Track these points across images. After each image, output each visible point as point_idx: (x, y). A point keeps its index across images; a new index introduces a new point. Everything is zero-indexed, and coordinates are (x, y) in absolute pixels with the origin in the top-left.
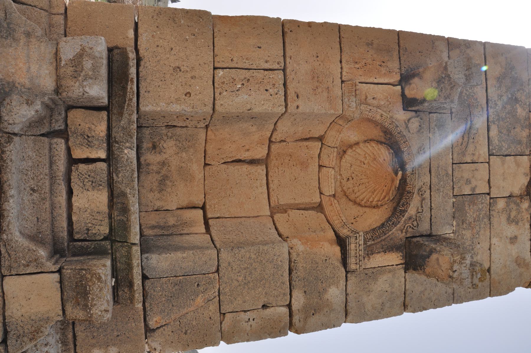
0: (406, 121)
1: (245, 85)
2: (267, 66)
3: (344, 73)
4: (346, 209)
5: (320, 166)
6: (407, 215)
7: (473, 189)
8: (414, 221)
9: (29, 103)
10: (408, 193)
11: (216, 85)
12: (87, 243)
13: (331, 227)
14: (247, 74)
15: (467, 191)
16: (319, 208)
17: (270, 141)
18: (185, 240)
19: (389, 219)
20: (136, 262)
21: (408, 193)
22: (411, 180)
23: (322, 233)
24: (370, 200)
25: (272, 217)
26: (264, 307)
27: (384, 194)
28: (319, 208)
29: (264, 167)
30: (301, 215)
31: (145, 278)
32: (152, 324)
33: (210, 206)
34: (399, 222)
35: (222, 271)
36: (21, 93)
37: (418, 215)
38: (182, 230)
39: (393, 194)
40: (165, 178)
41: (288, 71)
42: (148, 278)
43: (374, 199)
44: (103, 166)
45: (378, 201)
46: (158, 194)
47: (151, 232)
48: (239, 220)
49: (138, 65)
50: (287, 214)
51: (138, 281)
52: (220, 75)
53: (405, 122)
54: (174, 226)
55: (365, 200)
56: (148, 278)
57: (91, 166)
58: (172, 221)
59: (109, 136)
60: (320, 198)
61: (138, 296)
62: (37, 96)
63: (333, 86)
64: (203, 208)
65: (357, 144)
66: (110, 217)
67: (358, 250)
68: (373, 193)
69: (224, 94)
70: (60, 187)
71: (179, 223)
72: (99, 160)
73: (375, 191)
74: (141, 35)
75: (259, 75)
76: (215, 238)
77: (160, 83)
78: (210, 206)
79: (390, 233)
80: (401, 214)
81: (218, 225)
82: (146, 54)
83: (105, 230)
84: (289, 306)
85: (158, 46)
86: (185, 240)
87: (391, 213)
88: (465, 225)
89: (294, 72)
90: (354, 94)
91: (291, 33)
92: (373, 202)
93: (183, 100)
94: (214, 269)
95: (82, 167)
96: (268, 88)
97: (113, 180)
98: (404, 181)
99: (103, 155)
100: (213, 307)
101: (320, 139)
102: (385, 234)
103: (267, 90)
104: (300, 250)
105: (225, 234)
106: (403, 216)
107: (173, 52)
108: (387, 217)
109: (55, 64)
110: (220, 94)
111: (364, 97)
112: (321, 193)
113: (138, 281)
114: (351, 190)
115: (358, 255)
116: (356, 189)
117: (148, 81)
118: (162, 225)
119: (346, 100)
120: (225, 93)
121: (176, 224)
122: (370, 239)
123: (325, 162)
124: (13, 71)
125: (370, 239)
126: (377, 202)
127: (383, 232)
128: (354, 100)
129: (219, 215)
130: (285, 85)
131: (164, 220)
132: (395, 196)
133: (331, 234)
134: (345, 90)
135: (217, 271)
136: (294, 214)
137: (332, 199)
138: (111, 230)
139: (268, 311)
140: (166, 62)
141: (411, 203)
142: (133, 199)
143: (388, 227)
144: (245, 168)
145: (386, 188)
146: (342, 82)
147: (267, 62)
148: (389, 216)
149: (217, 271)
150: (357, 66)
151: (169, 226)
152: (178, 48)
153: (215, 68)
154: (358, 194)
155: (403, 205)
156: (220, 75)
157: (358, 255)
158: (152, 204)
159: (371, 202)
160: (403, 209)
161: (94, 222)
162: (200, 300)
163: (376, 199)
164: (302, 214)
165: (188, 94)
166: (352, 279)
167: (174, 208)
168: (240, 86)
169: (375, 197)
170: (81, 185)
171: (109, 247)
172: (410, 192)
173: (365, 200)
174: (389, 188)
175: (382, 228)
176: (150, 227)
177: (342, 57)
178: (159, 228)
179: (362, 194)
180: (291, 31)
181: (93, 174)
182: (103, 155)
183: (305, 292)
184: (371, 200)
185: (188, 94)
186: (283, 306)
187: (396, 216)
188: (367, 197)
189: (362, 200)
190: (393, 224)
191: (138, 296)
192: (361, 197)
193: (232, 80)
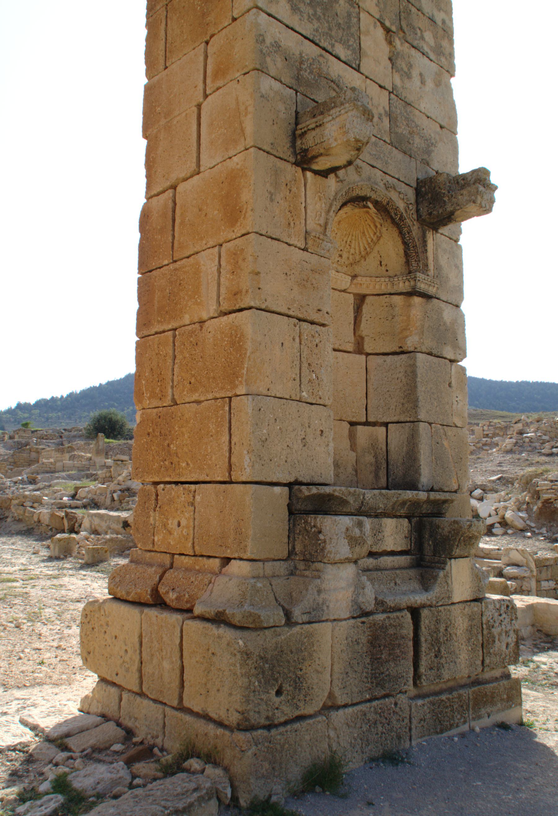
0: (338, 180)
1: (313, 369)
3: (299, 245)
4: (368, 270)
8: (409, 208)
10: (388, 204)
11: (314, 402)
12: (413, 538)
13: (388, 296)
14: (305, 365)
16: (361, 299)
18: (396, 449)
19: (401, 233)
21: (388, 204)
22: (380, 195)
23: (397, 309)
24: (370, 242)
25: (367, 354)
27: (372, 226)
28: (361, 299)
30: (368, 322)
33: (353, 417)
34: (409, 226)
35: (431, 421)
36: (358, 595)
37: (405, 201)
38: (381, 449)
39: (378, 218)
42: (433, 487)
43: (370, 237)
45: (375, 234)
46: (341, 469)
47: (382, 480)
48: (371, 390)
50: (366, 338)
52: (306, 396)
53: (338, 182)
54: (376, 456)
55: (367, 247)
56: (433, 487)
58: (369, 458)
60: (350, 293)
62: (359, 580)
63: (310, 263)
64: (352, 424)
67: (427, 282)
68: (365, 235)
69: (321, 394)
70: (382, 561)
71: (372, 451)
73: (364, 233)
74: (278, 478)
76: (395, 419)
77: (315, 461)
78: (353, 417)
79: (416, 240)
80: (403, 221)
81: (376, 413)
82: (294, 475)
85: (286, 461)
86: (396, 449)
87: (395, 229)
89: (301, 309)
90: (321, 242)
91: (268, 301)
92: (372, 240)
93: (326, 439)
96: (315, 343)
97: (382, 512)
98: (376, 204)
102: (416, 246)
103: (317, 345)
104: (417, 340)
105: (389, 409)
106: (405, 219)
107: (290, 445)
108: (397, 234)
109: (339, 565)
110: (320, 398)
112: (344, 291)
114: (351, 257)
115: (430, 283)
116: (352, 251)
117: (314, 474)
118: (374, 468)
119: (322, 252)
120: (320, 393)
121: (373, 454)
122: (418, 264)
124: (345, 602)
125: (418, 264)
126: (375, 236)
127: (413, 247)
128: (325, 243)
129: (364, 410)
131: (368, 465)
132: (381, 216)
134: (314, 250)
135: (430, 424)
136: (365, 328)
137: (355, 281)
139: (453, 383)
140: (299, 453)
141: (397, 205)
142: (403, 495)
143: (410, 239)
145: (368, 221)
147: (294, 339)
148: (397, 231)
150: (292, 224)
151: (376, 462)
152: (287, 439)
154: (357, 252)
155: (396, 215)
156: (306, 396)
157: (430, 283)
158: (350, 476)
159: (371, 241)
160: (399, 216)
161: (402, 531)
163: (372, 235)
164: (367, 320)
168: (314, 375)
169: (369, 234)
170: (380, 542)
171: (415, 519)
172: (389, 201)
173: (367, 247)
174: (370, 218)
175: (408, 246)
176: (376, 480)
177: (284, 241)
178: (378, 472)
179: (359, 247)
180: (266, 301)
181: (374, 532)
183: (445, 344)
184: (369, 240)
186: (451, 367)
187: (403, 226)
188: (365, 242)
189: (366, 249)
190: (408, 233)
192: (362, 249)
193: (310, 383)
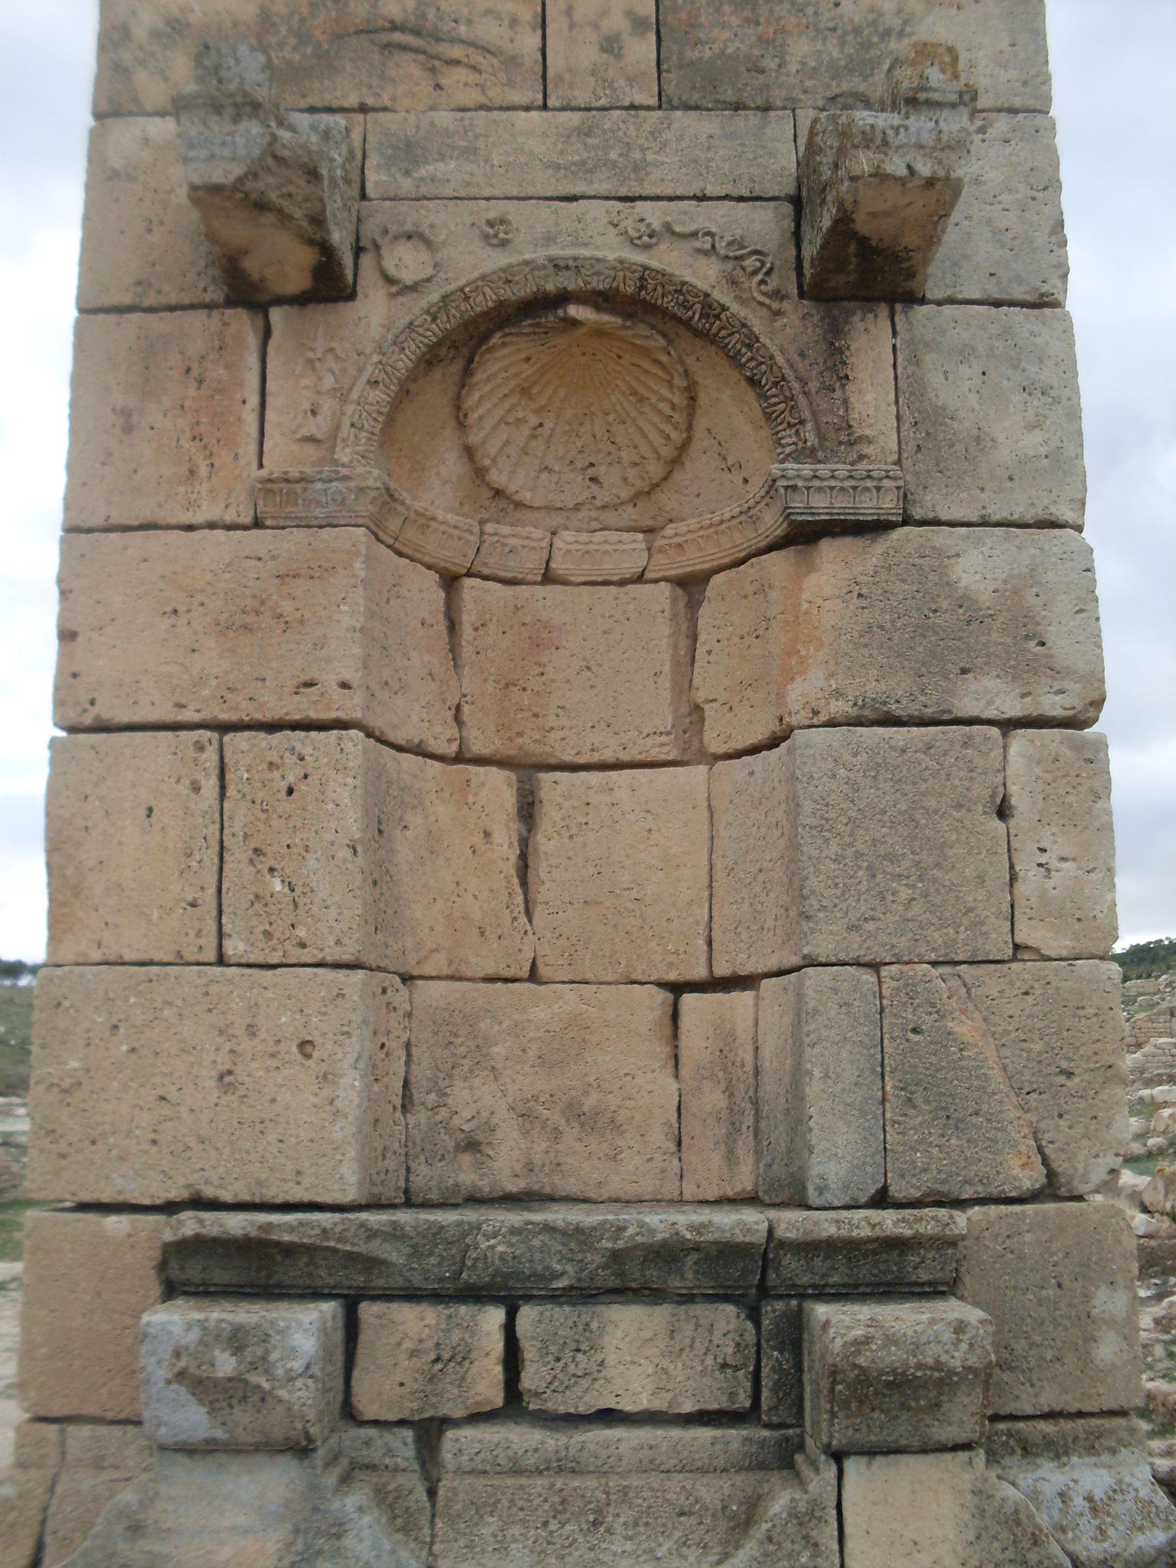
0: (394, 289)
1: (272, 863)
2: (210, 785)
3: (229, 517)
4: (698, 495)
5: (548, 578)
6: (721, 296)
7: (638, 24)
8: (743, 269)
9: (337, 1529)
11: (275, 958)
12: (765, 1371)
13: (754, 560)
14: (238, 855)
15: (643, 50)
17: (460, 758)
19: (734, 359)
20: (826, 1225)
21: (642, 288)
24: (669, 412)
26: (1003, 811)
27: (646, 364)
29: (546, 778)
30: (712, 658)
31: (881, 1200)
32: (1030, 1178)
34: (744, 325)
37: (722, 252)
39: (646, 337)
40: (574, 1112)
41: (226, 716)
42: (885, 1188)
43: (662, 399)
44: (527, 1315)
45: (670, 385)
46: (627, 1135)
48: (720, 875)
49: (215, 1205)
50: (706, 707)
51: (889, 1221)
52: (242, 947)
54: (729, 1092)
55: (668, 429)
56: (885, 1188)
57: (529, 1350)
58: (713, 1099)
59: (436, 1297)
61: (928, 1221)
63: (273, 558)
64: (678, 989)
65: (469, 452)
66: (688, 1299)
67: (833, 483)
68: (642, 400)
71: (721, 1074)
72: (510, 1329)
73: (635, 393)
75: (239, 814)
77: (272, 1137)
78: (671, 965)
79: (780, 359)
80: (718, 317)
81: (732, 947)
82: (181, 1181)
83: (727, 1316)
84: (1008, 725)
88: (770, 63)
90: (298, 487)
91: (98, 703)
92: (673, 404)
94: (868, 977)
95: (529, 1379)
96: (284, 785)
97: (572, 1288)
99: (496, 1316)
100: (990, 981)
101: (450, 581)
102: (783, 378)
103: (290, 791)
104: (821, 683)
106: (724, 308)
107: (173, 1095)
110: (303, 945)
111: (311, 450)
112: (640, 578)
113: (889, 1221)
114: (631, 473)
116: (627, 455)
117: (264, 1176)
118: (724, 1131)
120: (301, 932)
121: (723, 1085)
123: (532, 563)
125: (797, 433)
129: (701, 943)
130: (272, 727)
131: (710, 1121)
132: (653, 327)
133: (778, 563)
135: (875, 966)
138: (726, 1298)
139: (1018, 800)
144: (547, 843)
146: (257, 524)
147: (196, 788)
149: (875, 966)
150: (203, 471)
152: (158, 1080)
153: (221, 960)
154: (645, 450)
159: (673, 408)
160: (698, 307)
161: (700, 1348)
162: (964, 1028)
163: (665, 392)
164: (709, 652)
165: (305, 1046)
166: (932, 503)
167: (674, 1086)
169: (656, 393)
170: (584, 1383)
171: (779, 1305)
172: (642, 278)
176: (730, 1169)
177: (173, 521)
178: (734, 1140)
181: (553, 1349)
182: (496, 1316)
183: (964, 671)
185: (305, 1046)
186: (1005, 748)
187: (723, 333)
188: (656, 420)
189: (668, 437)
190: (749, 347)
191: (928, 1221)
192: (658, 440)
